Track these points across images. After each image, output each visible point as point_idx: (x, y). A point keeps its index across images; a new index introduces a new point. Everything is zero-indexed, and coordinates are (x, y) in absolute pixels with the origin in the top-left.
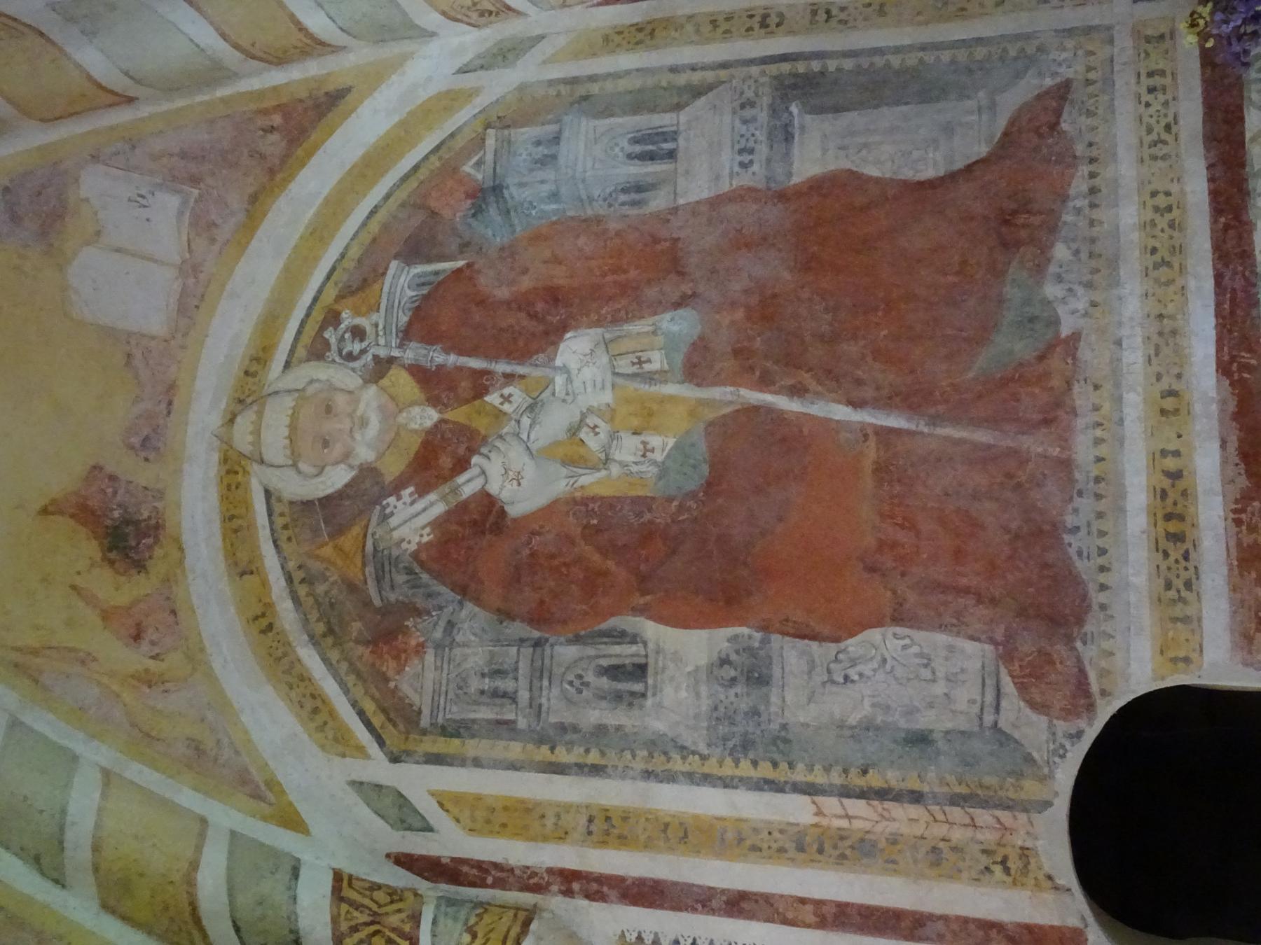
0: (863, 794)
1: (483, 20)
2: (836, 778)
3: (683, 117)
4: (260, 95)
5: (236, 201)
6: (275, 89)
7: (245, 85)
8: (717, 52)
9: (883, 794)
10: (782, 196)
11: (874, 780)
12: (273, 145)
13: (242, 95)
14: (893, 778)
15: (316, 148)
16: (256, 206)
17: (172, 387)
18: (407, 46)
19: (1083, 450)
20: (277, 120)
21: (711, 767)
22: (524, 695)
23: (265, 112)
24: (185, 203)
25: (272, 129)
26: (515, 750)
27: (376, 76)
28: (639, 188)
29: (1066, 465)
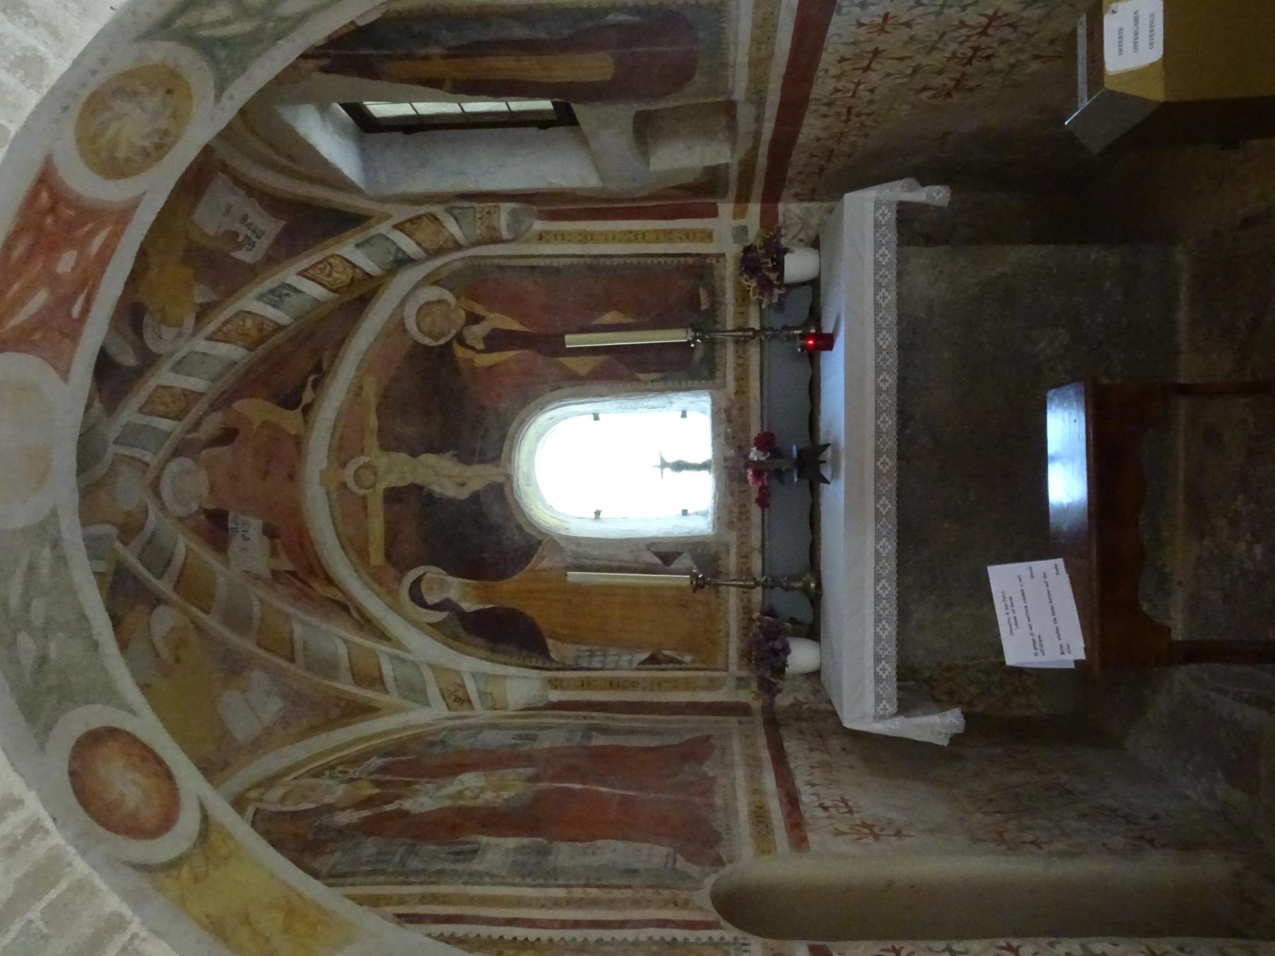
0: (597, 887)
1: (454, 705)
2: (582, 882)
3: (542, 732)
4: (343, 692)
5: (305, 722)
6: (349, 693)
7: (339, 686)
8: (562, 721)
9: (608, 886)
10: (586, 748)
11: (605, 882)
12: (335, 712)
13: (336, 688)
14: (614, 882)
15: (354, 723)
16: (312, 730)
17: (227, 765)
18: (414, 705)
19: (719, 801)
20: (343, 704)
21: (509, 880)
22: (397, 859)
23: (339, 698)
24: (284, 708)
25: (337, 706)
26: (381, 878)
27: (395, 710)
28: (515, 745)
29: (711, 806)
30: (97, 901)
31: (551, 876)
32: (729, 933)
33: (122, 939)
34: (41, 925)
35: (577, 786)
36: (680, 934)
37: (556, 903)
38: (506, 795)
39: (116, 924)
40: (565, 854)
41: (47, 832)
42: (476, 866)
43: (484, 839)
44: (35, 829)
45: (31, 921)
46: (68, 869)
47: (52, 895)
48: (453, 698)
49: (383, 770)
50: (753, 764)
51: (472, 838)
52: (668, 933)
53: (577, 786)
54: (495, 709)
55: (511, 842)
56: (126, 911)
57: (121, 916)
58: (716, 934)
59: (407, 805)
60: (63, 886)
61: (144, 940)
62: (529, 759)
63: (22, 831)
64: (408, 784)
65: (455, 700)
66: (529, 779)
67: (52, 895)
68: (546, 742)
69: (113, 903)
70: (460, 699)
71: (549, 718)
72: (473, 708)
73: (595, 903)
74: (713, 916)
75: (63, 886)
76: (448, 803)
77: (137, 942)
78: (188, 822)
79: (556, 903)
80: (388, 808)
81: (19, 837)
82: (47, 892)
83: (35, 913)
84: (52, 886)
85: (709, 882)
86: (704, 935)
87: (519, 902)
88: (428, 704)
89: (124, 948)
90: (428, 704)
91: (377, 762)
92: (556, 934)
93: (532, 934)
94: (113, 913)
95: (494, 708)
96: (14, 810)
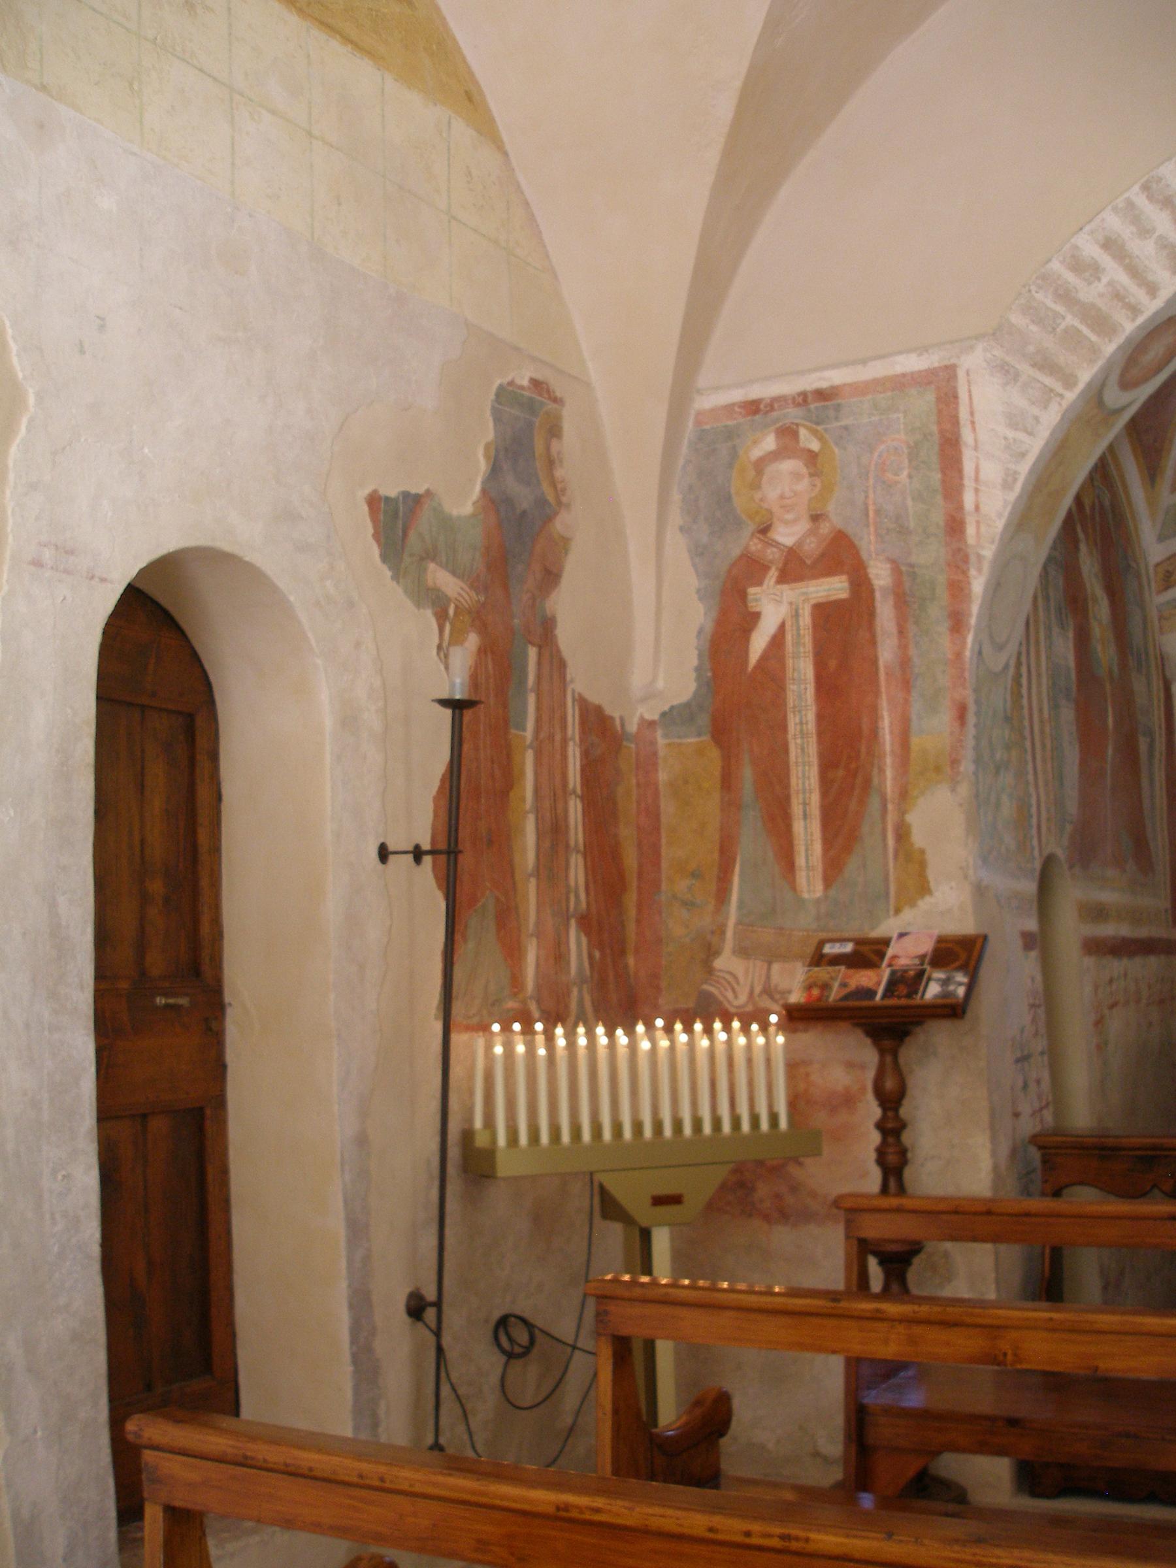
27: (1152, 503)
30: (1085, 365)
31: (1055, 707)
32: (1038, 865)
33: (1058, 387)
34: (1063, 326)
35: (1110, 721)
36: (1034, 821)
37: (1041, 710)
38: (1099, 648)
39: (1069, 382)
40: (1068, 714)
41: (1133, 320)
42: (1056, 630)
43: (1071, 635)
44: (1134, 310)
45: (1064, 318)
46: (1107, 340)
47: (1086, 331)
48: (1170, 569)
49: (1102, 506)
50: (1135, 916)
51: (1071, 622)
52: (1034, 810)
53: (1110, 721)
54: (1160, 620)
55: (1072, 664)
56: (1081, 386)
57: (1075, 384)
58: (1036, 853)
59: (1083, 547)
60: (1094, 338)
61: (1060, 404)
62: (1123, 666)
63: (1133, 301)
64: (1096, 545)
65: (1168, 571)
66: (1110, 672)
67: (1086, 331)
68: (1138, 685)
69: (1085, 376)
70: (1169, 577)
71: (1157, 685)
72: (1159, 592)
73: (1043, 745)
74: (1046, 853)
75: (1094, 338)
76: (1089, 590)
77: (1058, 399)
78: (1125, 398)
79: (1041, 710)
80: (1079, 529)
81: (1127, 300)
82: (1088, 326)
83: (1071, 320)
84: (1093, 330)
85: (1061, 854)
86: (1035, 842)
87: (1039, 675)
88: (1161, 538)
89: (1051, 390)
90: (1161, 538)
91: (1107, 503)
92: (1026, 711)
93: (1024, 691)
94: (1076, 377)
95: (1161, 618)
96: (1148, 293)
